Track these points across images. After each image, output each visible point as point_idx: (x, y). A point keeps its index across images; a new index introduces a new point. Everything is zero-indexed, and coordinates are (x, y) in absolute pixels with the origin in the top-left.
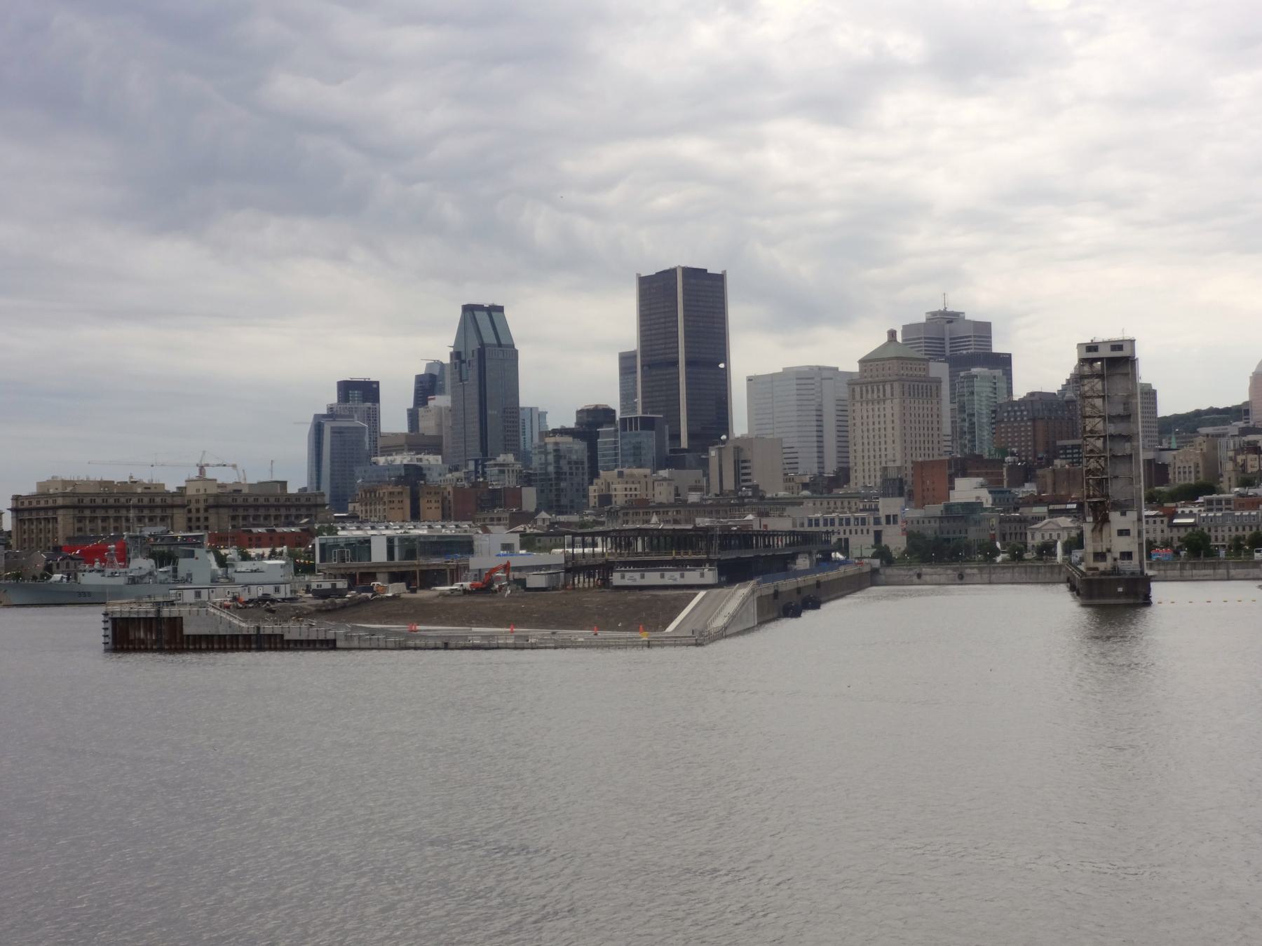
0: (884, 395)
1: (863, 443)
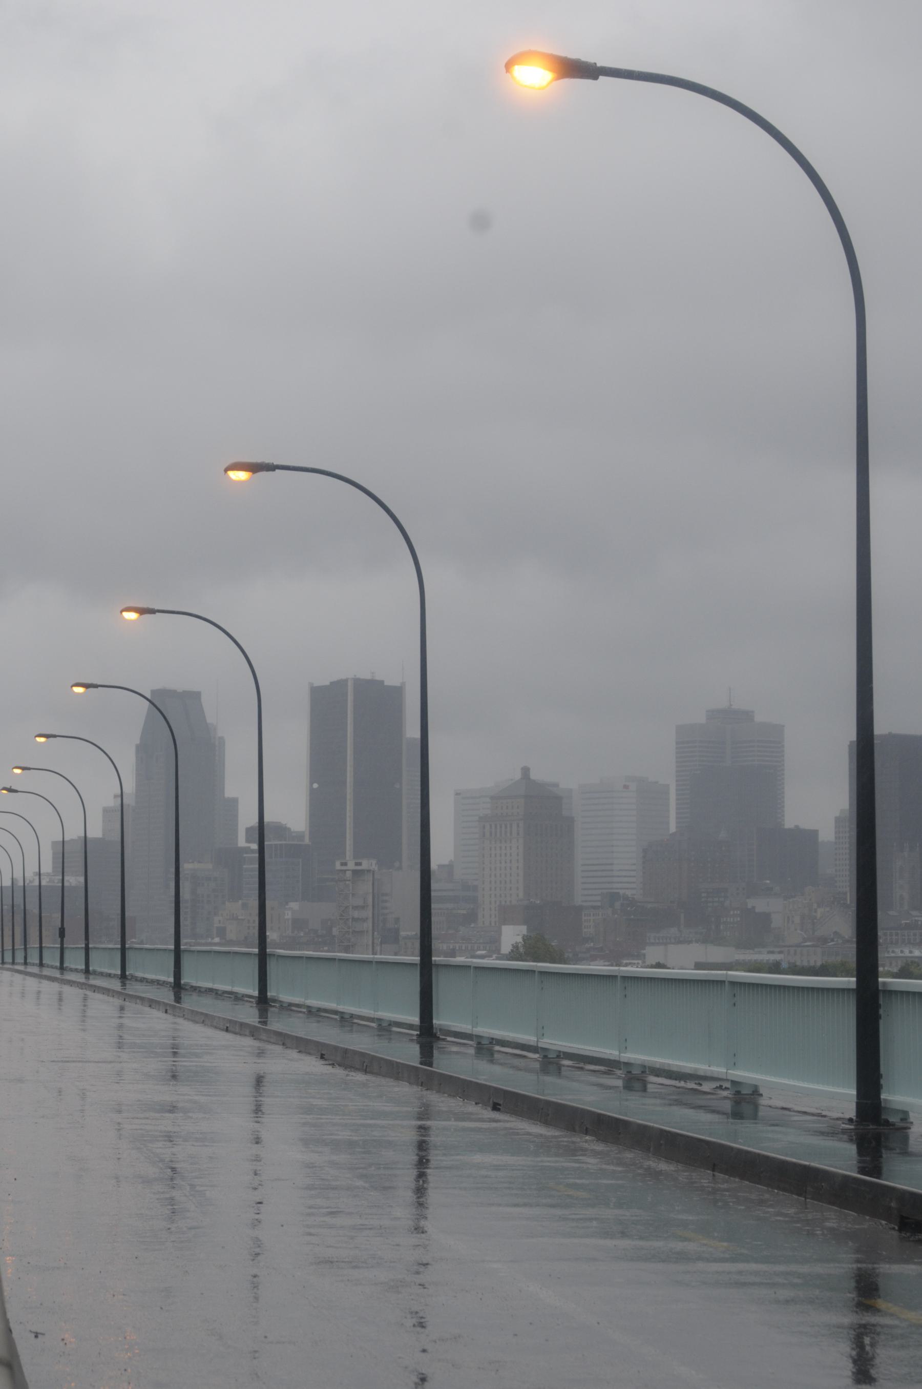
0: (511, 834)
1: (490, 882)
